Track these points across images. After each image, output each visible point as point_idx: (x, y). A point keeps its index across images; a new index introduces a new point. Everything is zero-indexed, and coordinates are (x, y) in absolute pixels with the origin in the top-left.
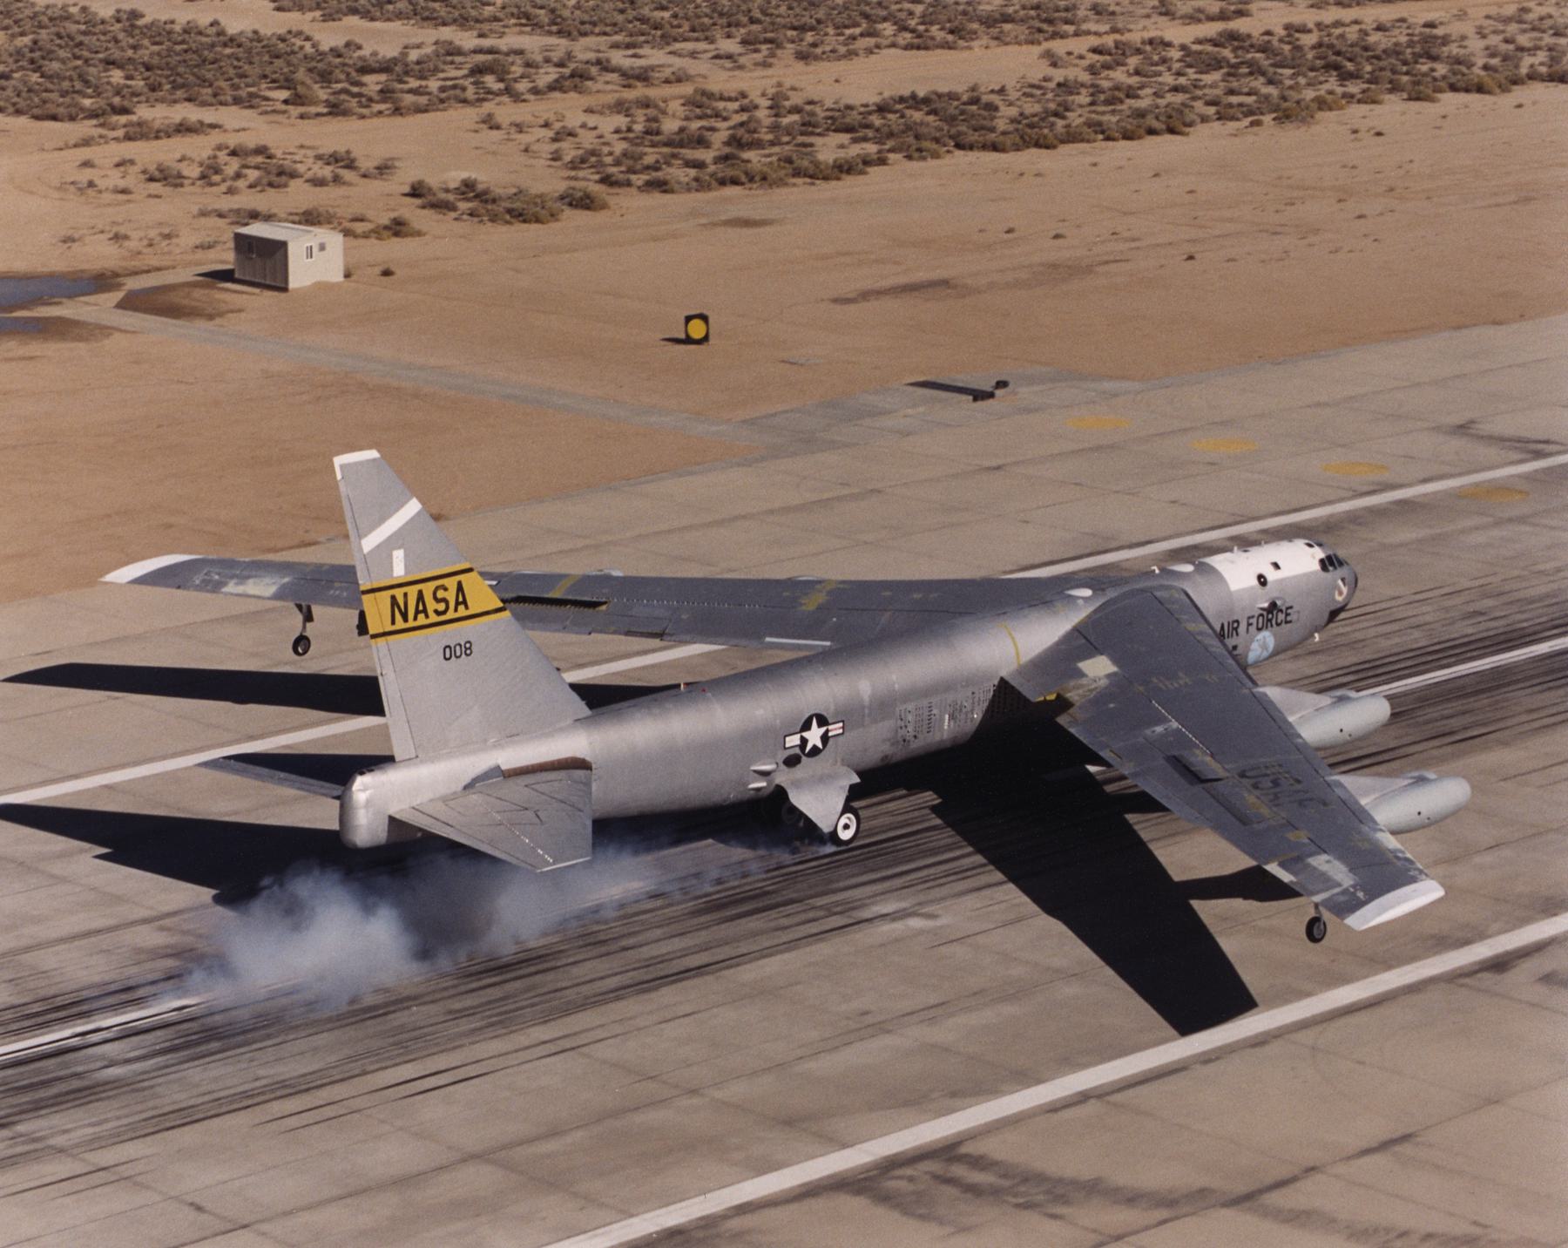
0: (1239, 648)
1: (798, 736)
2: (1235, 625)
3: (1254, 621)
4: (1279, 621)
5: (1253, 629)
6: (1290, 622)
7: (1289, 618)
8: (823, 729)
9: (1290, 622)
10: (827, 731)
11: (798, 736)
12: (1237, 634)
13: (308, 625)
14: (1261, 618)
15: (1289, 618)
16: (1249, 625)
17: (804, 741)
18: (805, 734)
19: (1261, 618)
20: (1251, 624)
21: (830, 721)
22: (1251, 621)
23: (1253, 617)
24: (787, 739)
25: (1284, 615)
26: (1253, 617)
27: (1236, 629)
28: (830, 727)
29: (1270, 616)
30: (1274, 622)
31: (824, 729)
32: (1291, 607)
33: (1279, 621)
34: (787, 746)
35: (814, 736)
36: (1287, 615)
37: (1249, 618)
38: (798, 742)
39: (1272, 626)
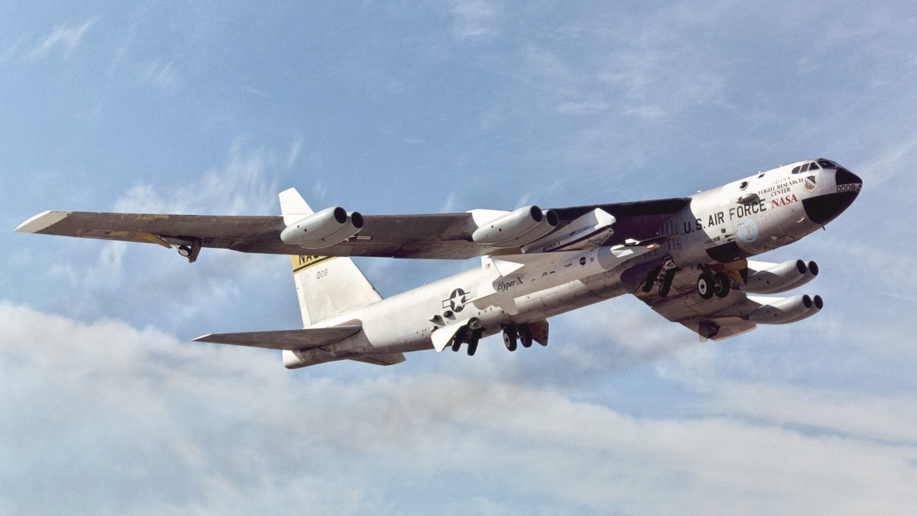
0: (726, 230)
1: (449, 301)
2: (721, 215)
3: (735, 211)
4: (755, 210)
5: (735, 216)
6: (765, 209)
7: (763, 207)
8: (462, 297)
9: (765, 209)
10: (464, 297)
11: (450, 300)
12: (723, 222)
13: (499, 337)
14: (740, 209)
15: (763, 207)
16: (731, 214)
17: (453, 304)
18: (453, 300)
19: (740, 209)
20: (733, 214)
21: (465, 292)
22: (732, 212)
23: (734, 209)
24: (444, 302)
25: (759, 205)
26: (734, 209)
27: (722, 218)
28: (466, 295)
29: (747, 207)
30: (751, 210)
31: (462, 297)
32: (764, 200)
33: (755, 210)
34: (444, 306)
35: (458, 301)
36: (761, 205)
37: (730, 210)
38: (450, 304)
39: (750, 214)
